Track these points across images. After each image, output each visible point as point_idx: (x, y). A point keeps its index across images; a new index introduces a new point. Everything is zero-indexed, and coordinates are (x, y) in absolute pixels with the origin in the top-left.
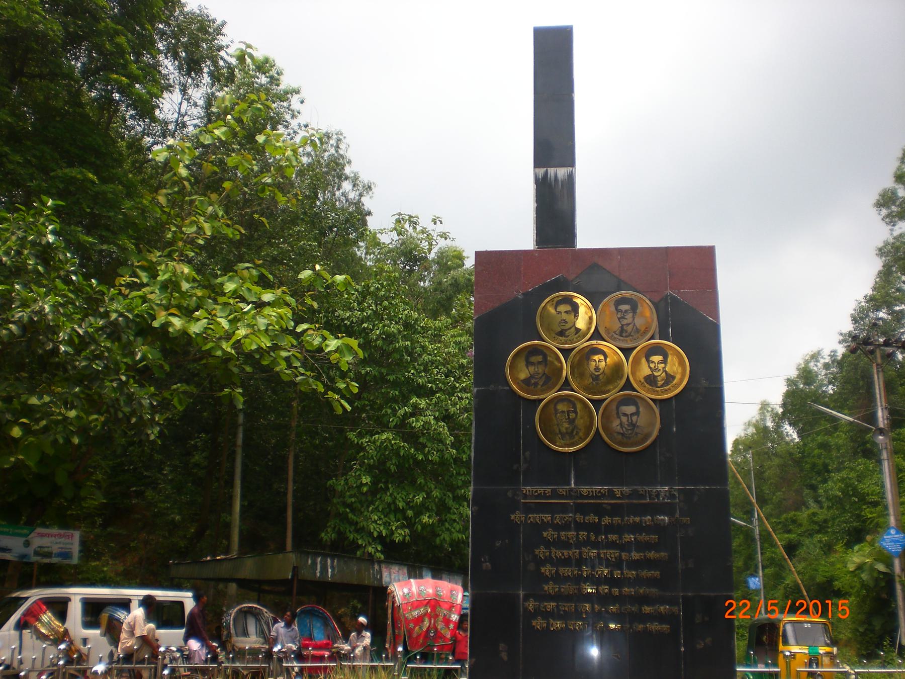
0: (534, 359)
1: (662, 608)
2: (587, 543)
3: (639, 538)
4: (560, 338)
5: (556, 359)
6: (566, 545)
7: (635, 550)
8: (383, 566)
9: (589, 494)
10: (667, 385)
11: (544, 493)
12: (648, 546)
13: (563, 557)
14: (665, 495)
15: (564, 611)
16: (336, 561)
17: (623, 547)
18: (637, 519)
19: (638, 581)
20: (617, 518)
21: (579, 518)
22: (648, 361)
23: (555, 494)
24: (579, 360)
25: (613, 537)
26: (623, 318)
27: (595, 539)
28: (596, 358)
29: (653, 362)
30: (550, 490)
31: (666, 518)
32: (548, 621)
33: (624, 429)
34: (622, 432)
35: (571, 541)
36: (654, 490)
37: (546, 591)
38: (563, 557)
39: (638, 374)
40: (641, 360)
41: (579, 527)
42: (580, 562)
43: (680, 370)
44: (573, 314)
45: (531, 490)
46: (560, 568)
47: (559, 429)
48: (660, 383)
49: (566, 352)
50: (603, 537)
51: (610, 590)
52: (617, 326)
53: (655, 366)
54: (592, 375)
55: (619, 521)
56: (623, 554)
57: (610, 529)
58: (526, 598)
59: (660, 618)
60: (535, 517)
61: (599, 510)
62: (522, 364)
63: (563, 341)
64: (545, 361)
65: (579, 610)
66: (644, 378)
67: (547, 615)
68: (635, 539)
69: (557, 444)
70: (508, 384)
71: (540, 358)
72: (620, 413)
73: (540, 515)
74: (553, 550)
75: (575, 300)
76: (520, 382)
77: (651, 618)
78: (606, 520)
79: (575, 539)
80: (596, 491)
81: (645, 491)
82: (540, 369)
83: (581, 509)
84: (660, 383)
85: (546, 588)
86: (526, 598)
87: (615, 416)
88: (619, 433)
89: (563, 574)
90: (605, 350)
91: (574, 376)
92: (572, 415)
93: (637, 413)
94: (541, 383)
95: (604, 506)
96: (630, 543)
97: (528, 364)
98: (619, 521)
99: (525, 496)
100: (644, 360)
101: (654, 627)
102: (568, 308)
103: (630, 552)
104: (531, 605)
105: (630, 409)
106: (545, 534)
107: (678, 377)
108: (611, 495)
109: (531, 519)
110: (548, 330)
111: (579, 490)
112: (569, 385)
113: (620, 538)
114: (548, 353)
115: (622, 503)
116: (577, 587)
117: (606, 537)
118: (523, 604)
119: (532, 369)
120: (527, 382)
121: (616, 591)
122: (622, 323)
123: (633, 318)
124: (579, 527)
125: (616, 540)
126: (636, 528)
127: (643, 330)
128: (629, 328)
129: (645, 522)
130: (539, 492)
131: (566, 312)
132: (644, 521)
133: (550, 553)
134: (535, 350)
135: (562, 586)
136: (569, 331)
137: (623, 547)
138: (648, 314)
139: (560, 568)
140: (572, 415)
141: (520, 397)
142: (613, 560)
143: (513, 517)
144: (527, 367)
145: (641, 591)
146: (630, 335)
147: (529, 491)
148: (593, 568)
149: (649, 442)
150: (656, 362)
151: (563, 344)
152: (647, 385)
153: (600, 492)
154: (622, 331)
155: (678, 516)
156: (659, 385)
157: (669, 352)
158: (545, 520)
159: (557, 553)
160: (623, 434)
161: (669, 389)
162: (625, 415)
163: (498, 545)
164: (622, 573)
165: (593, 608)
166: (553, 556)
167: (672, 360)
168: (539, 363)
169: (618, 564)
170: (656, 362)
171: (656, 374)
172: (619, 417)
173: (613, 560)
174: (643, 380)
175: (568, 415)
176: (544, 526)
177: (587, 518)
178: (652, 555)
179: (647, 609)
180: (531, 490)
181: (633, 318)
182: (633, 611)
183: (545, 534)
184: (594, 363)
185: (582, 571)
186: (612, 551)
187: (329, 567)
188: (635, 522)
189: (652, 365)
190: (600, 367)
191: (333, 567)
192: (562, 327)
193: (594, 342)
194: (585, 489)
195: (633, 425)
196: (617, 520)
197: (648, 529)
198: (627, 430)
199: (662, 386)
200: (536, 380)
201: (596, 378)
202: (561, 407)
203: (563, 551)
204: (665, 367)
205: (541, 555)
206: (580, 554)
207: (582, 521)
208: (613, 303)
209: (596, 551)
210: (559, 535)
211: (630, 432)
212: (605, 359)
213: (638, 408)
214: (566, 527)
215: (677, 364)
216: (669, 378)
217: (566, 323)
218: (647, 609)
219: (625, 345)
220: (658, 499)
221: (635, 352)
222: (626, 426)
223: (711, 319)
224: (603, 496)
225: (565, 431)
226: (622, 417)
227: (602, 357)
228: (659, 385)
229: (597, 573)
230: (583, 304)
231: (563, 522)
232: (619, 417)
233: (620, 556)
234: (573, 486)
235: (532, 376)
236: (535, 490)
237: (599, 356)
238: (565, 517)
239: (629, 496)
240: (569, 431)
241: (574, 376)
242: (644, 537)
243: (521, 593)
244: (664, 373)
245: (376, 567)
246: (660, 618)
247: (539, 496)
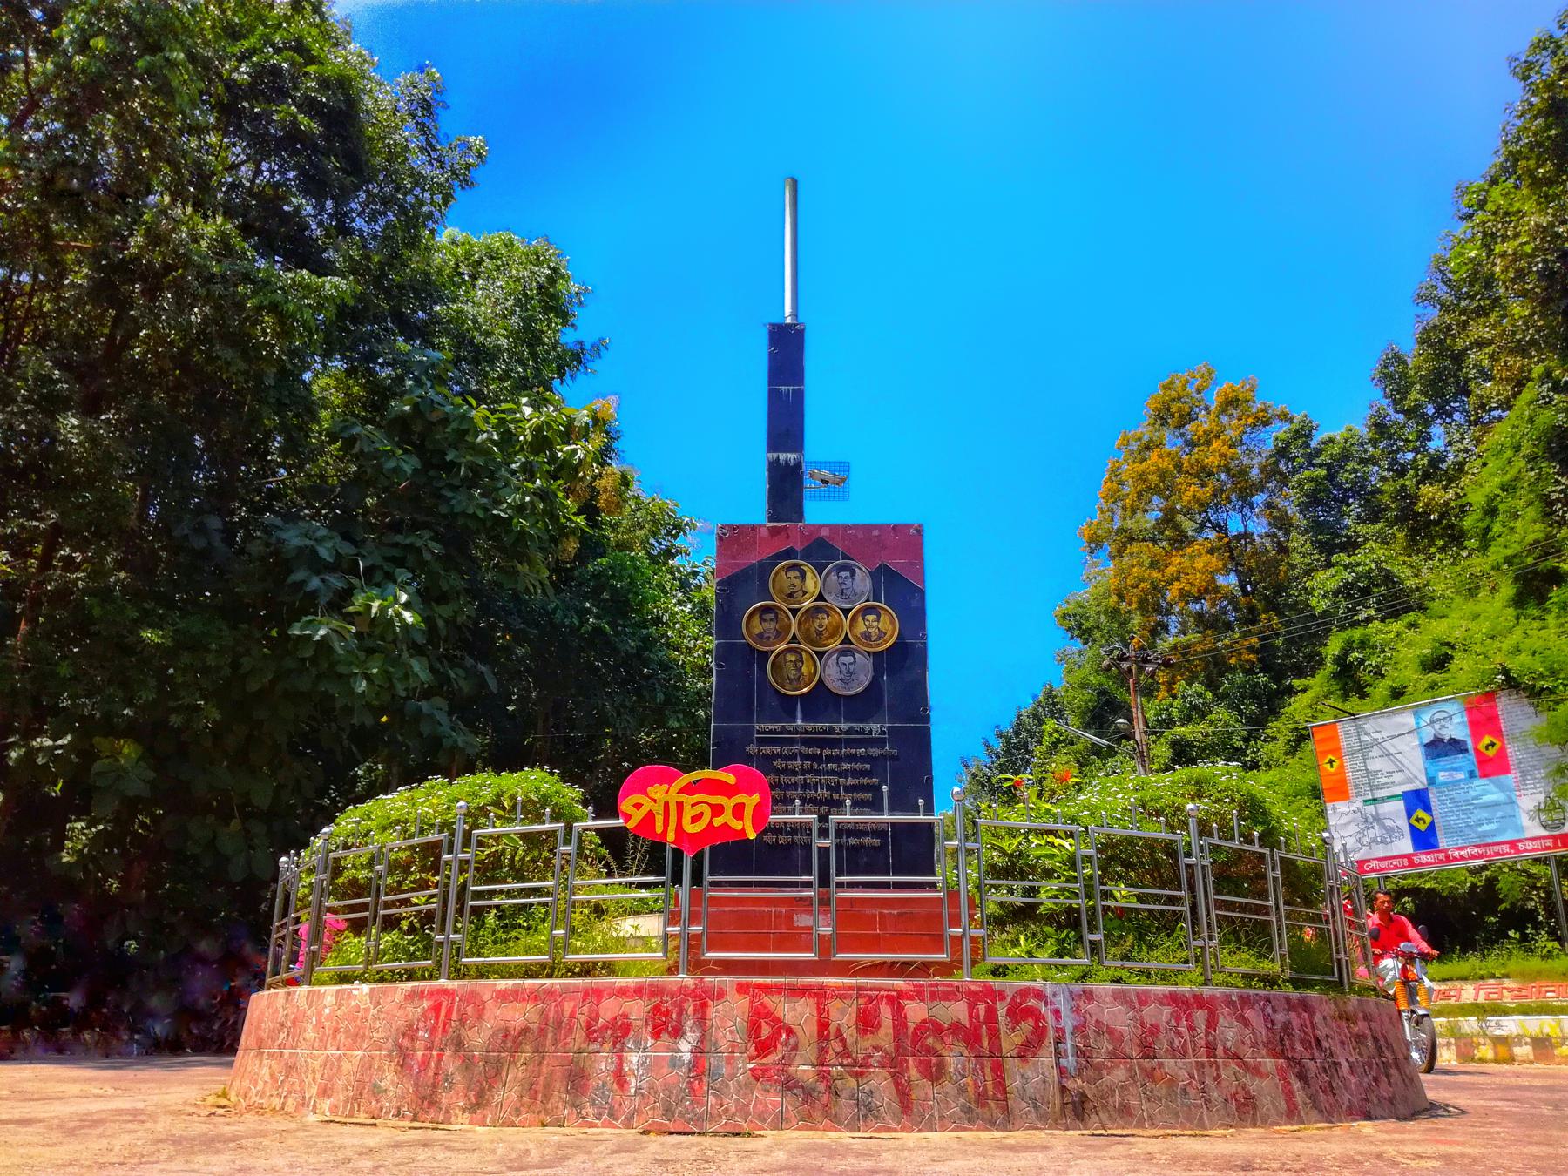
0: (767, 617)
2: (810, 771)
6: (794, 773)
12: (863, 773)
21: (804, 750)
41: (805, 757)
49: (794, 612)
57: (830, 759)
61: (823, 743)
62: (756, 620)
78: (827, 752)
83: (807, 743)
97: (762, 620)
103: (847, 778)
110: (781, 592)
120: (761, 636)
124: (805, 757)
126: (852, 758)
128: (848, 593)
137: (840, 774)
157: (882, 612)
178: (865, 781)
194: (810, 726)
197: (863, 759)
201: (820, 634)
202: (791, 657)
216: (882, 634)
239: (847, 733)
242: (859, 766)
247: (771, 732)
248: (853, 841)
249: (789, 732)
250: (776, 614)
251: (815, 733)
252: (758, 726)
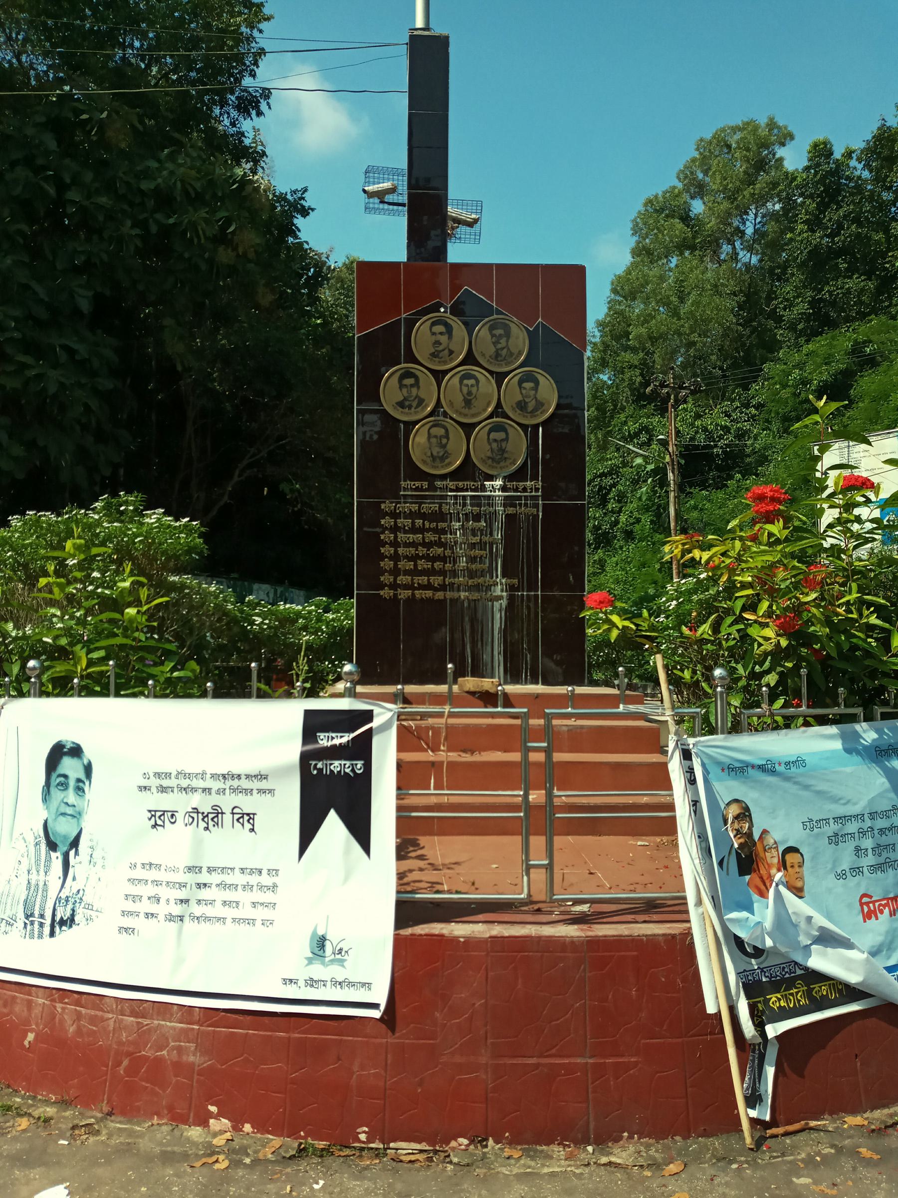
22: (520, 387)
29: (525, 388)
88: (489, 458)
92: (444, 441)
93: (507, 439)
120: (401, 404)
123: (507, 341)
131: (441, 333)
140: (444, 441)
146: (505, 359)
154: (497, 355)
168: (412, 386)
171: (527, 400)
174: (515, 406)
181: (507, 341)
189: (524, 392)
213: (507, 434)
217: (440, 344)
235: (405, 399)
240: (441, 454)
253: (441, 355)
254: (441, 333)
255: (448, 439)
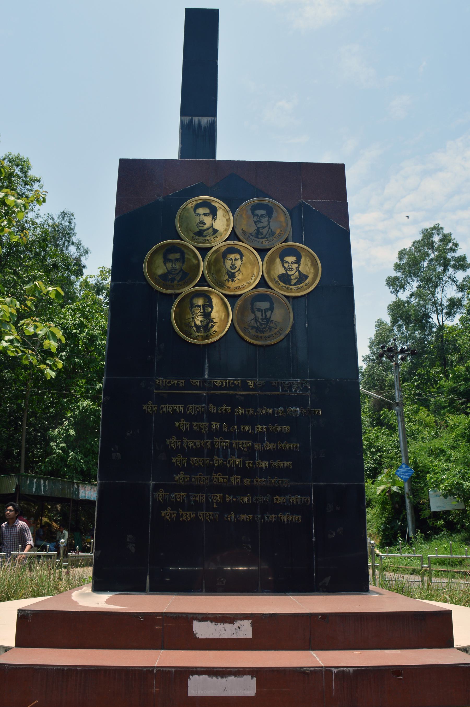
0: (173, 256)
1: (293, 497)
2: (220, 433)
3: (272, 428)
4: (198, 237)
5: (193, 257)
6: (198, 435)
7: (267, 440)
8: (80, 485)
9: (222, 384)
10: (300, 284)
11: (177, 383)
12: (280, 437)
13: (195, 447)
14: (298, 387)
15: (195, 501)
16: (47, 482)
17: (255, 438)
18: (270, 411)
19: (271, 472)
20: (251, 409)
21: (212, 408)
22: (283, 261)
23: (188, 386)
24: (215, 258)
25: (246, 428)
26: (259, 221)
27: (227, 429)
28: (232, 256)
30: (183, 381)
31: (298, 409)
32: (178, 511)
33: (258, 324)
34: (256, 326)
35: (203, 431)
36: (287, 382)
37: (177, 481)
38: (195, 447)
39: (272, 272)
40: (275, 260)
41: (212, 417)
42: (212, 452)
43: (312, 270)
44: (211, 216)
45: (164, 380)
46: (191, 458)
47: (195, 322)
48: (294, 282)
49: (204, 251)
50: (236, 427)
51: (242, 481)
52: (253, 229)
53: (289, 266)
54: (228, 272)
55: (252, 412)
56: (255, 444)
57: (243, 420)
58: (156, 488)
59: (293, 509)
60: (168, 408)
62: (159, 261)
63: (201, 240)
64: (183, 259)
65: (210, 500)
66: (278, 276)
67: (177, 506)
68: (267, 429)
69: (192, 336)
70: (145, 279)
71: (177, 256)
72: (254, 308)
73: (173, 405)
74: (185, 440)
75: (213, 204)
76: (157, 277)
77: (283, 508)
78: (240, 411)
79: (207, 429)
80: (229, 382)
81: (278, 383)
82: (178, 266)
84: (294, 282)
85: (177, 478)
86: (156, 488)
87: (250, 311)
88: (253, 327)
89: (194, 464)
90: (242, 249)
91: (211, 273)
94: (178, 279)
95: (237, 396)
96: (262, 433)
97: (166, 260)
98: (252, 412)
99: (158, 387)
100: (278, 260)
101: (286, 517)
102: (207, 211)
103: (262, 442)
104: (161, 495)
105: (265, 305)
106: (177, 424)
107: (311, 276)
108: (245, 386)
109: (164, 410)
110: (187, 230)
111: (212, 381)
112: (206, 281)
113: (253, 429)
114: (186, 251)
115: (254, 395)
116: (209, 477)
117: (239, 428)
118: (153, 495)
119: (169, 265)
120: (164, 277)
121: (247, 481)
122: (258, 226)
124: (212, 417)
125: (248, 431)
127: (278, 232)
128: (265, 231)
129: (278, 413)
130: (172, 383)
132: (276, 412)
133: (182, 442)
134: (173, 249)
135: (192, 476)
136: (206, 232)
137: (255, 438)
138: (282, 218)
139: (191, 458)
141: (156, 291)
142: (246, 449)
143: (145, 407)
144: (165, 264)
145: (273, 481)
147: (163, 381)
148: (225, 457)
149: (282, 337)
150: (290, 262)
151: (200, 243)
152: (282, 284)
153: (233, 383)
154: (258, 233)
155: (309, 407)
156: (292, 283)
157: (303, 254)
158: (178, 410)
159: (188, 443)
160: (257, 329)
161: (302, 287)
162: (259, 310)
163: (128, 434)
164: (254, 463)
165: (224, 498)
166: (185, 446)
167: (305, 260)
168: (177, 260)
169: (250, 454)
170: (290, 262)
171: (289, 273)
172: (254, 312)
173: (246, 449)
174: (277, 279)
175: (204, 309)
176: (177, 416)
177: (220, 408)
178: (284, 445)
179: (278, 499)
180: (164, 380)
182: (264, 501)
183: (177, 424)
184: (230, 262)
185: (213, 460)
186: (244, 441)
187: (42, 486)
188: (267, 413)
189: (286, 265)
190: (236, 265)
191: (44, 486)
192: (200, 228)
193: (231, 242)
195: (268, 320)
196: (250, 411)
198: (261, 324)
199: (295, 284)
200: (174, 276)
203: (194, 441)
204: (298, 267)
205: (172, 445)
206: (213, 443)
207: (215, 411)
208: (250, 208)
209: (229, 441)
210: (191, 426)
211: (264, 326)
212: (241, 258)
214: (198, 417)
215: (309, 265)
216: (302, 277)
217: (205, 224)
218: (278, 499)
219: (259, 246)
220: (291, 391)
221: (270, 253)
222: (260, 321)
223: (341, 226)
224: (236, 387)
225: (200, 324)
226: (256, 312)
227: (238, 256)
228: (292, 283)
229: (229, 463)
230: (220, 208)
231: (196, 412)
232: (254, 312)
233: (253, 446)
234: (206, 377)
235: (169, 272)
236: (168, 381)
237: (235, 255)
238: (197, 408)
241: (211, 273)
243: (151, 483)
244: (297, 273)
245: (75, 486)
246: (293, 509)
247: (173, 387)
248: (271, 517)
249: (196, 388)
250: (183, 254)
251: (226, 389)
252: (160, 380)
253: (205, 233)
254: (205, 215)
255: (212, 308)
